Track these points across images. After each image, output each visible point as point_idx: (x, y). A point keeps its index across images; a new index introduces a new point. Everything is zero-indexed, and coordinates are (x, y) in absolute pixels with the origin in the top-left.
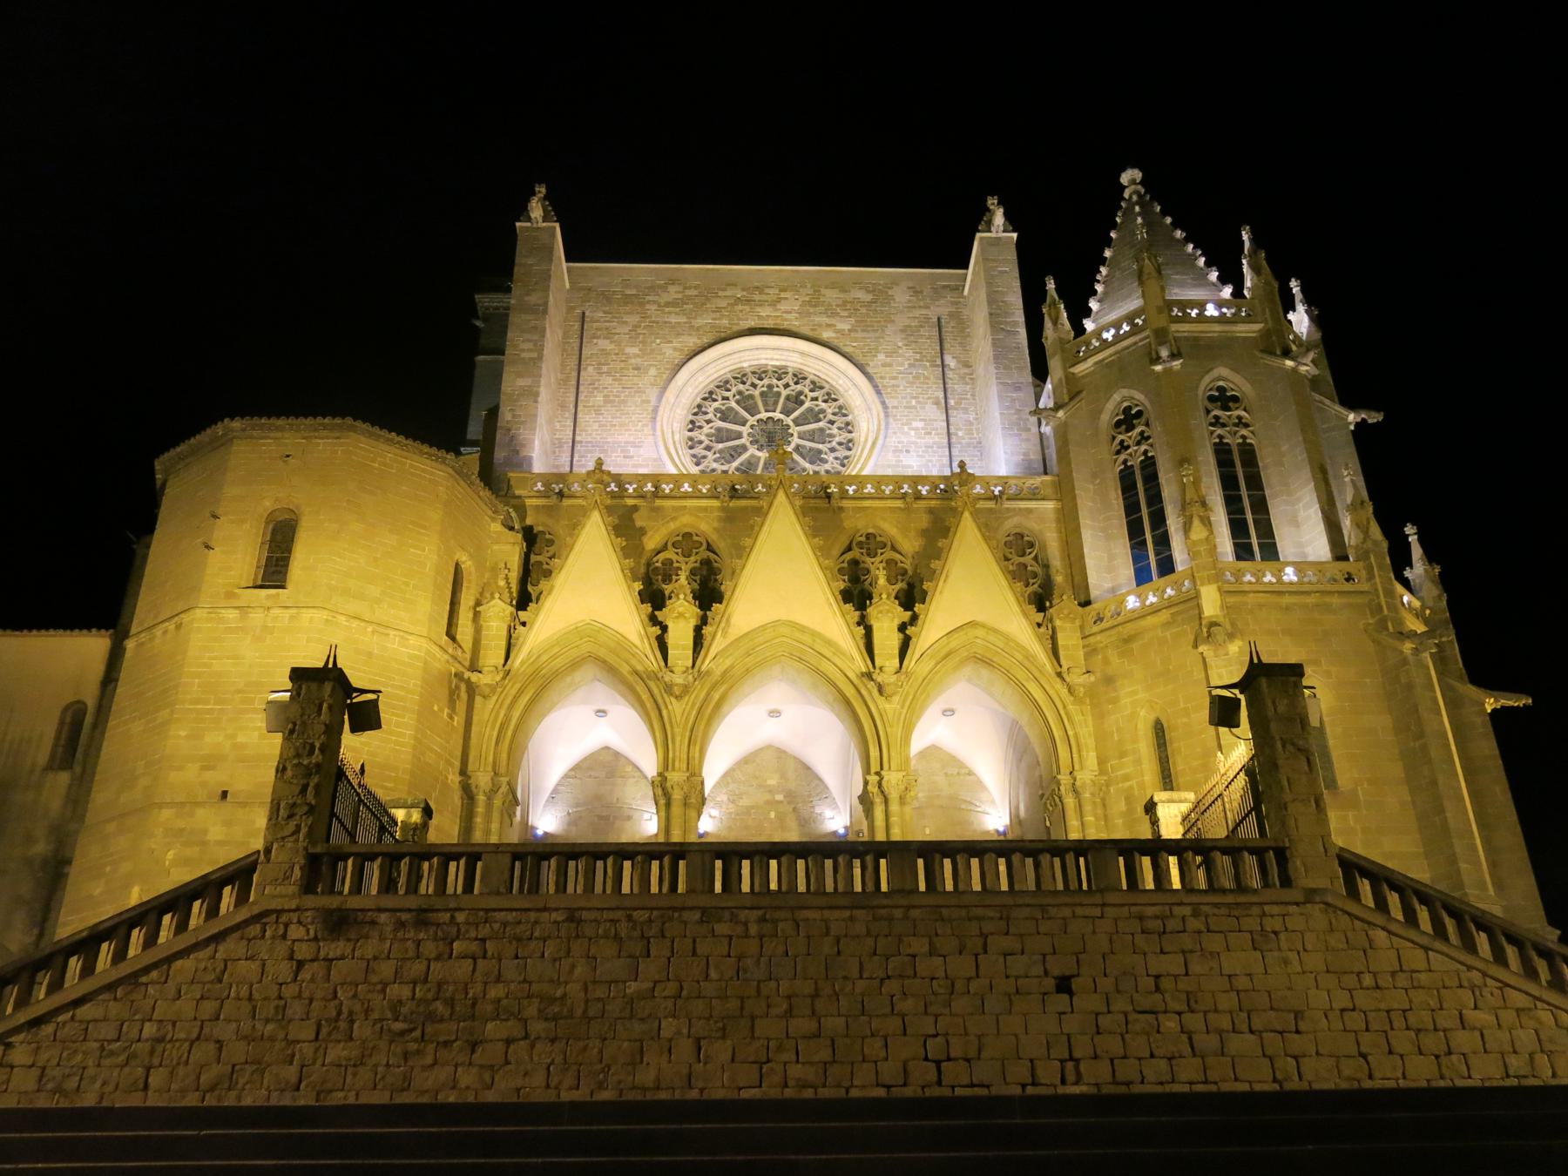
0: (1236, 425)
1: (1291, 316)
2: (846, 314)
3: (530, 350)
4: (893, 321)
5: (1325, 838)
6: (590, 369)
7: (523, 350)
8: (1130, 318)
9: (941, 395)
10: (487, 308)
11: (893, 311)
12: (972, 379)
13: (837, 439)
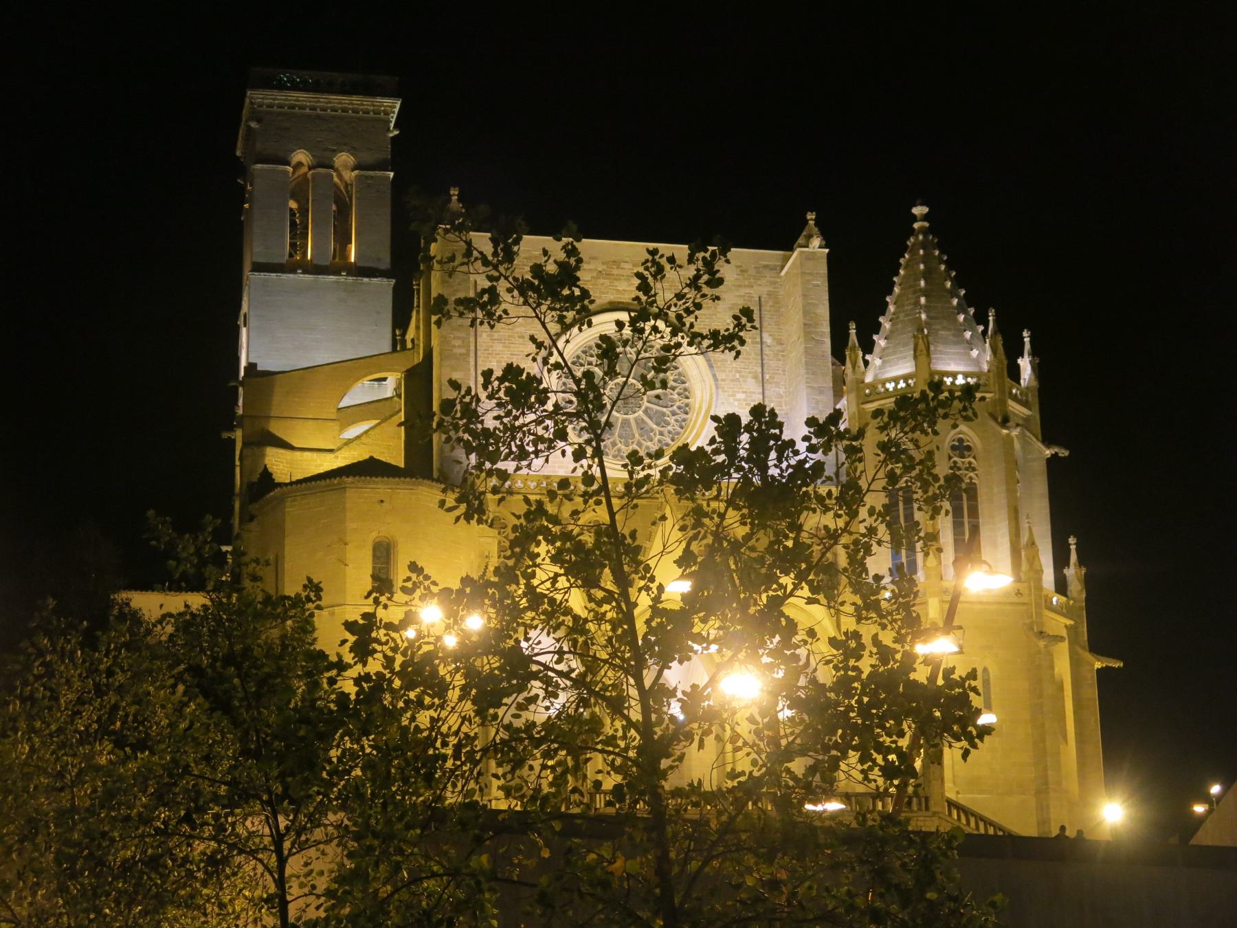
0: (967, 469)
1: (1020, 361)
5: (943, 794)
7: (454, 346)
8: (906, 378)
9: (760, 370)
10: (261, 105)
12: (783, 356)
13: (678, 404)
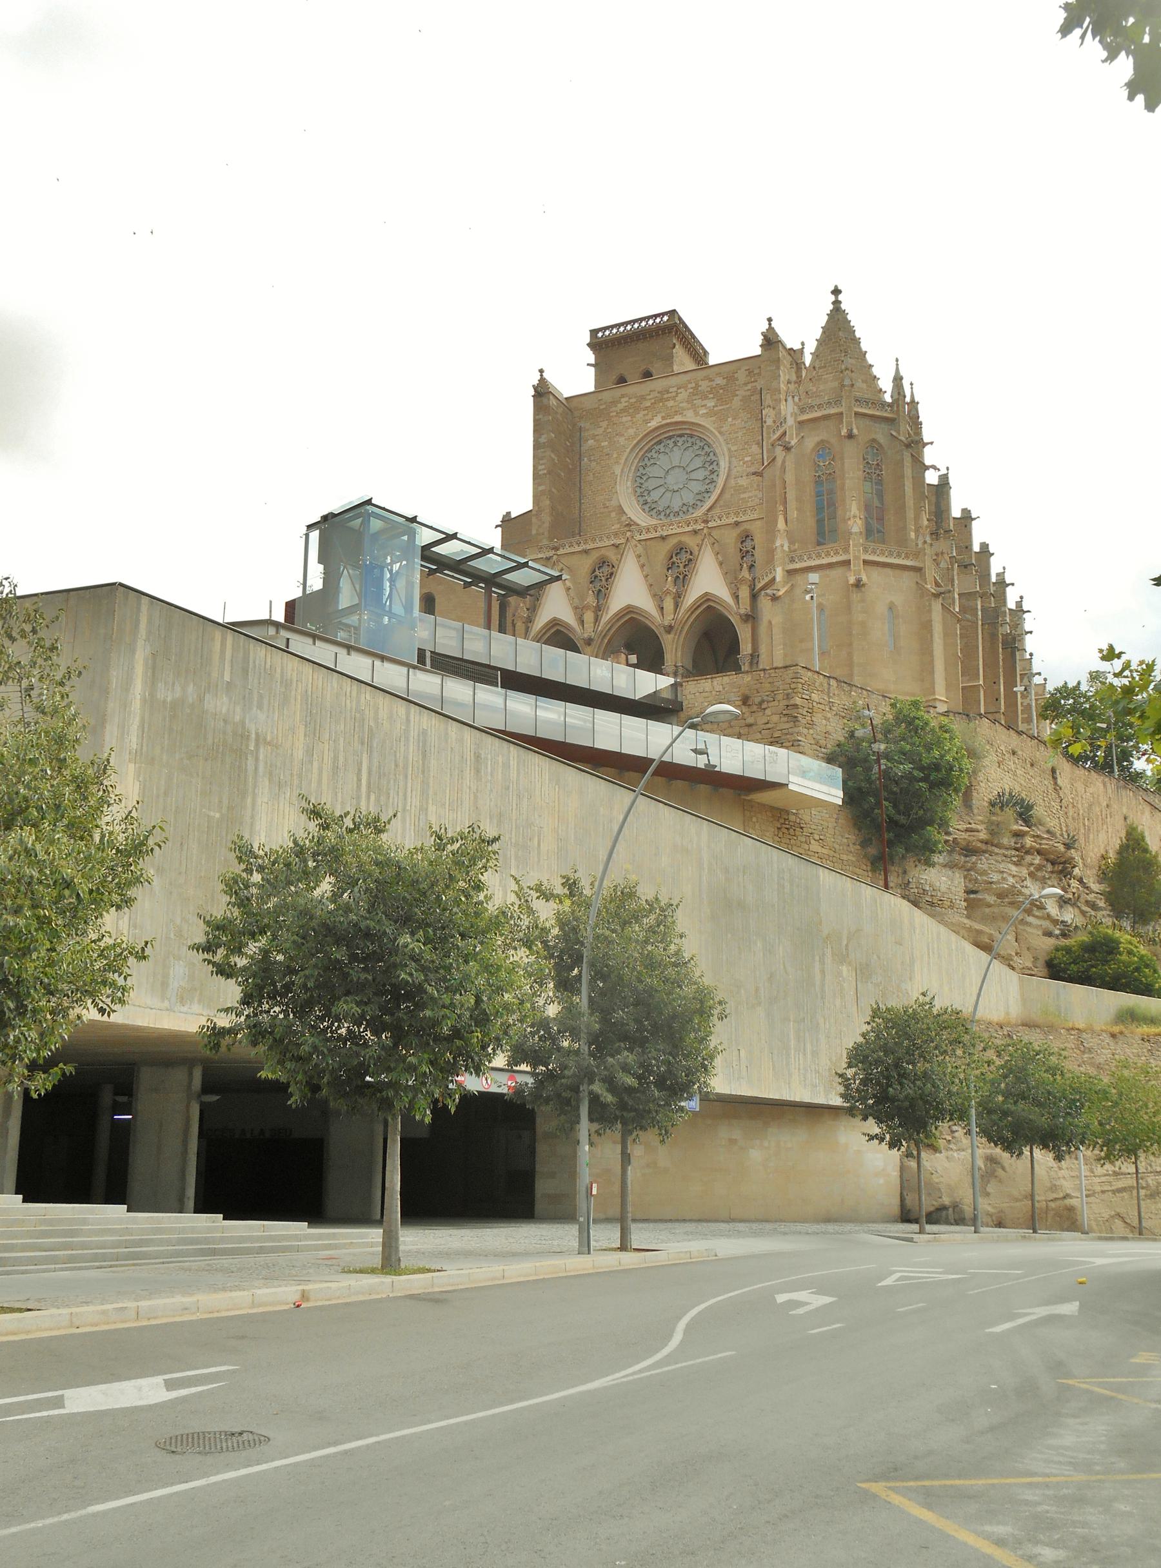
2: (712, 396)
3: (543, 469)
4: (737, 395)
6: (586, 459)
9: (761, 438)
11: (737, 388)
